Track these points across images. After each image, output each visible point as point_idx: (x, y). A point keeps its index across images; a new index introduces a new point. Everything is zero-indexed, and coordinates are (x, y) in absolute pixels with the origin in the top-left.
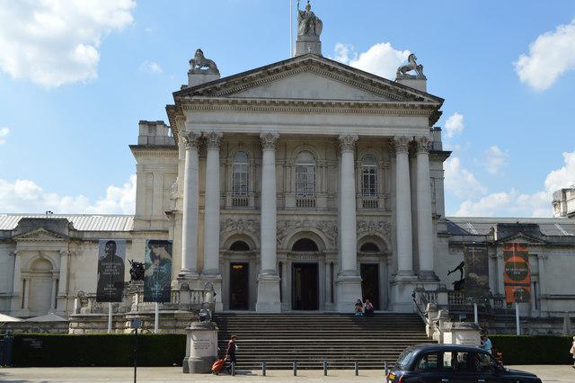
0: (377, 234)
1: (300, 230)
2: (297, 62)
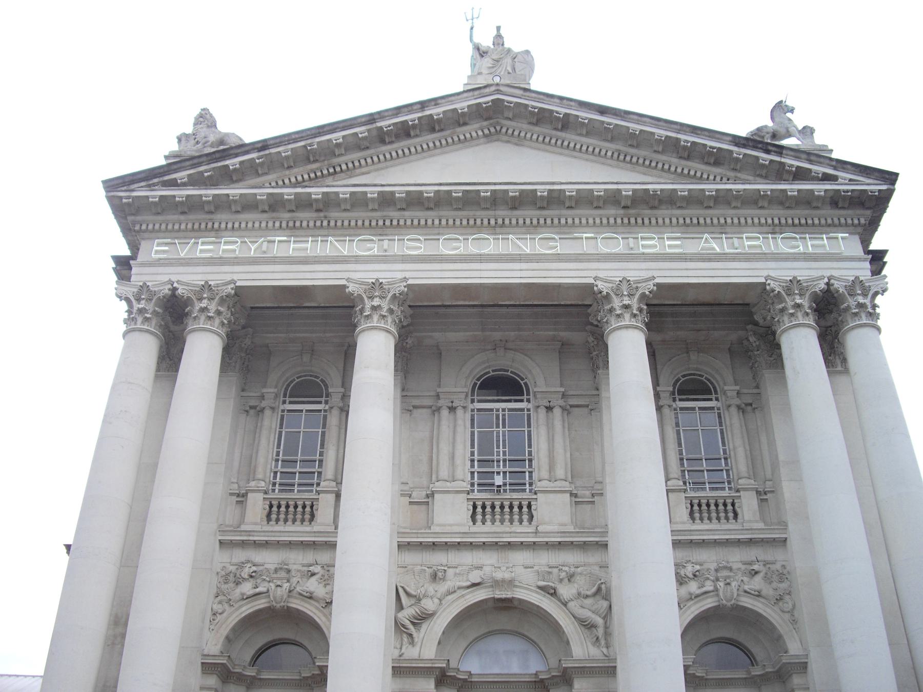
0: (747, 602)
1: (480, 595)
2: (462, 105)
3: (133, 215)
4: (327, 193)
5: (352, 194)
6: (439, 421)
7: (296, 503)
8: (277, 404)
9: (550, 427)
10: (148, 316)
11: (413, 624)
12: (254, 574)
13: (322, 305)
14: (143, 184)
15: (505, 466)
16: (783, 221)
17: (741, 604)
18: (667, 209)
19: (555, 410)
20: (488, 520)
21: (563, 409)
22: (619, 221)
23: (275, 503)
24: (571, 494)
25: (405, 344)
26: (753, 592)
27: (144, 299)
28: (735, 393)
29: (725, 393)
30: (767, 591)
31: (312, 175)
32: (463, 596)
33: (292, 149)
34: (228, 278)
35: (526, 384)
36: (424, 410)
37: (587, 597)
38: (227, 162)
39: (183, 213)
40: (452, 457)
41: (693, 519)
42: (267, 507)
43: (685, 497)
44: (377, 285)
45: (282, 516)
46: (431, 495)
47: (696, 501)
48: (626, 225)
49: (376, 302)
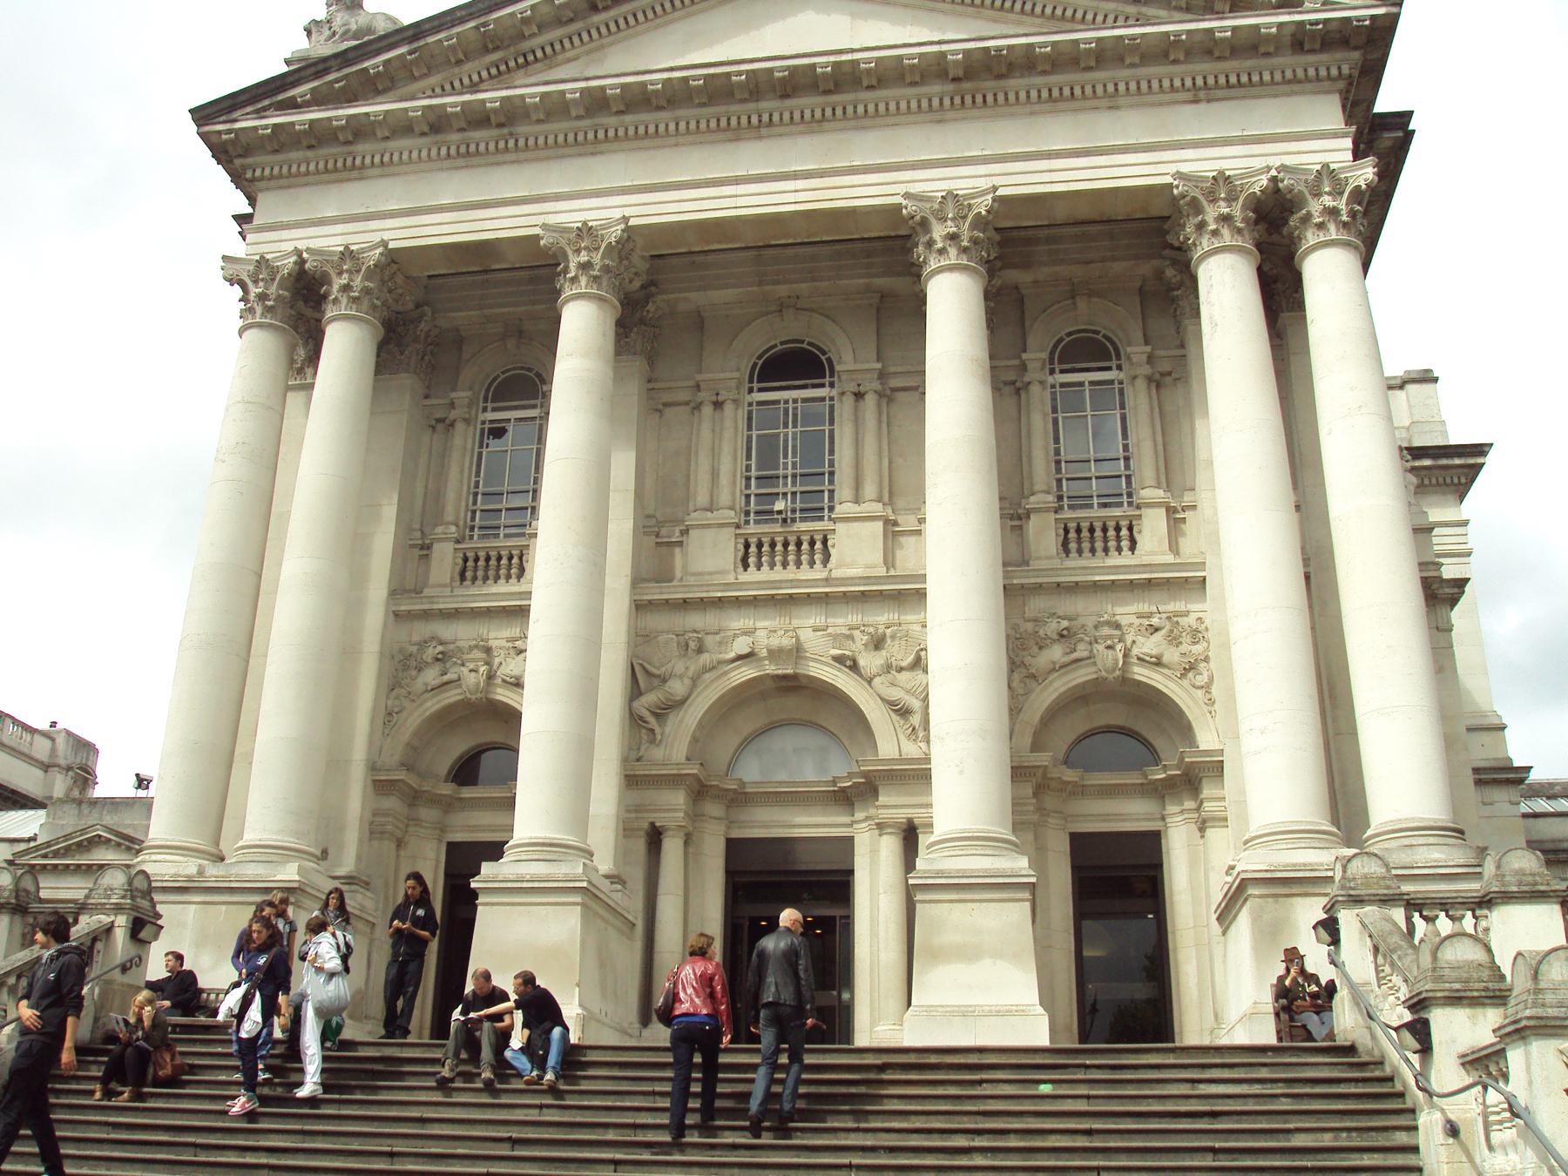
0: (1141, 673)
3: (241, 156)
4: (508, 98)
5: (544, 95)
6: (700, 422)
7: (499, 552)
8: (473, 412)
9: (857, 421)
10: (270, 303)
11: (656, 715)
12: (440, 656)
13: (517, 266)
14: (249, 109)
15: (794, 483)
16: (1211, 81)
17: (1130, 676)
18: (1022, 76)
19: (866, 397)
20: (765, 564)
21: (880, 395)
22: (947, 102)
23: (471, 555)
24: (889, 523)
25: (645, 314)
26: (1148, 659)
27: (262, 280)
28: (1144, 358)
29: (1129, 358)
30: (1171, 655)
31: (494, 71)
32: (726, 673)
33: (458, 34)
34: (376, 238)
35: (829, 360)
36: (682, 408)
37: (900, 670)
38: (366, 65)
39: (310, 147)
40: (715, 475)
41: (1067, 551)
42: (460, 561)
43: (1056, 519)
44: (585, 231)
45: (480, 573)
46: (685, 532)
47: (1072, 525)
48: (959, 107)
49: (584, 257)
